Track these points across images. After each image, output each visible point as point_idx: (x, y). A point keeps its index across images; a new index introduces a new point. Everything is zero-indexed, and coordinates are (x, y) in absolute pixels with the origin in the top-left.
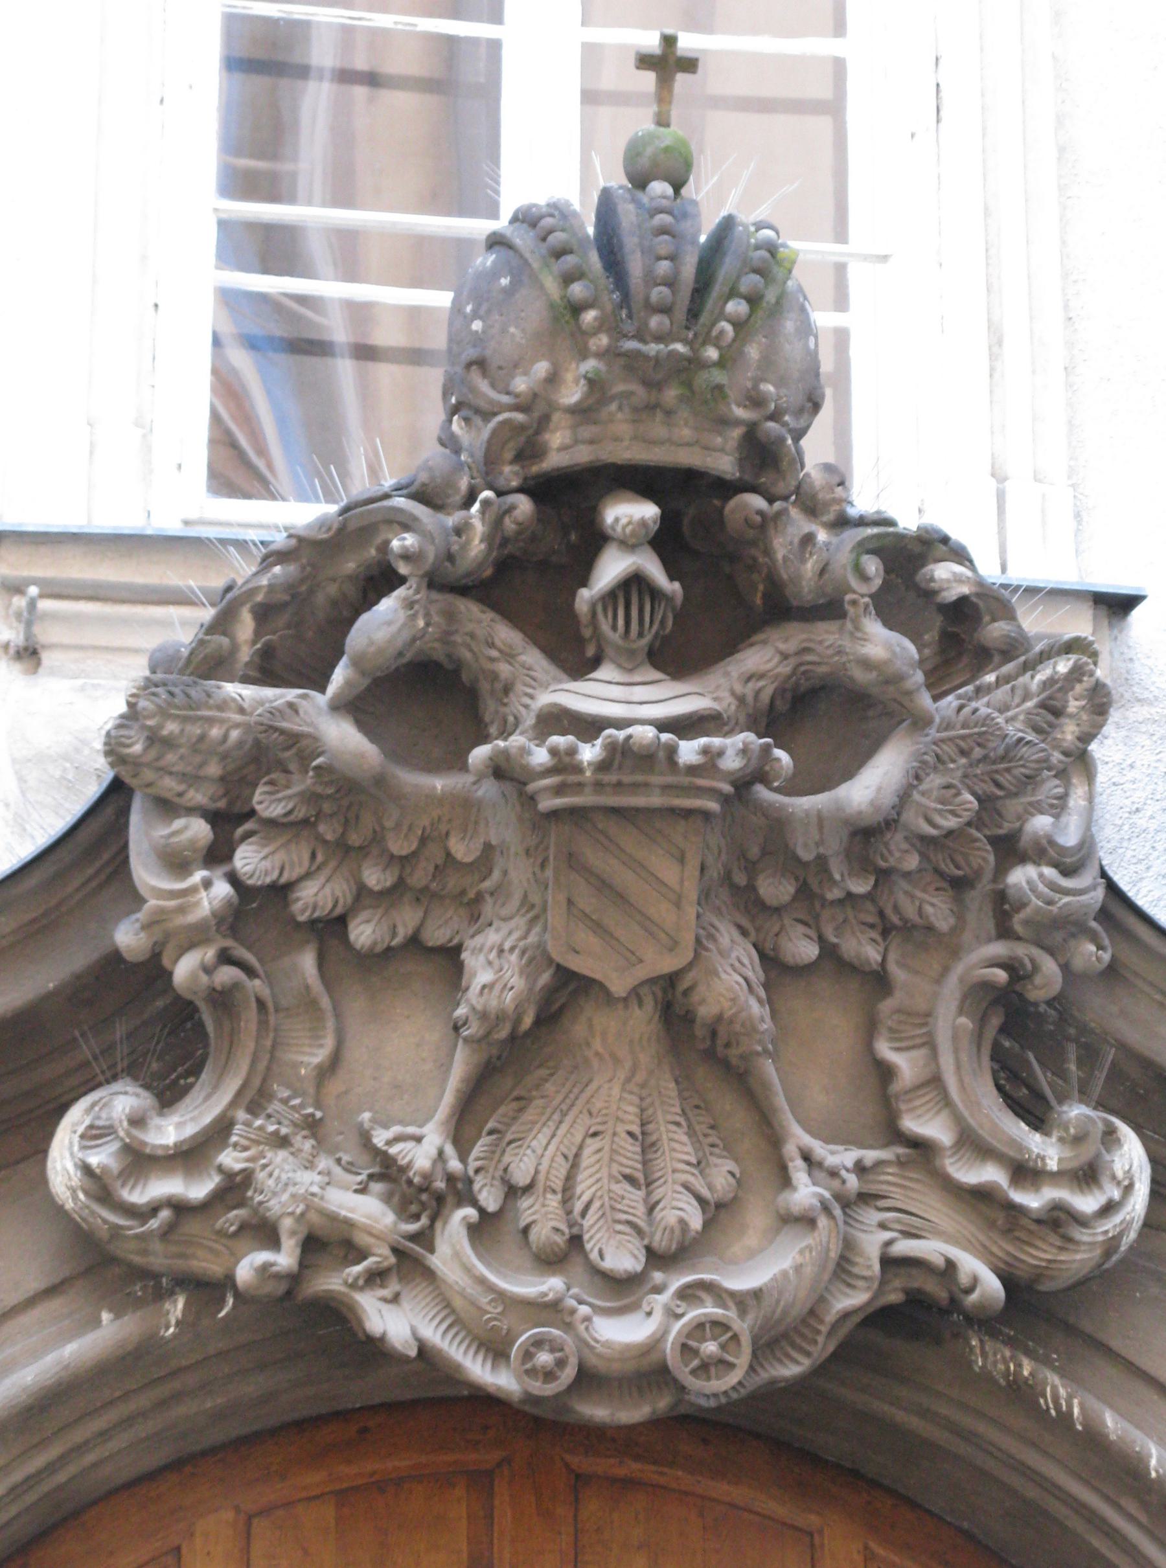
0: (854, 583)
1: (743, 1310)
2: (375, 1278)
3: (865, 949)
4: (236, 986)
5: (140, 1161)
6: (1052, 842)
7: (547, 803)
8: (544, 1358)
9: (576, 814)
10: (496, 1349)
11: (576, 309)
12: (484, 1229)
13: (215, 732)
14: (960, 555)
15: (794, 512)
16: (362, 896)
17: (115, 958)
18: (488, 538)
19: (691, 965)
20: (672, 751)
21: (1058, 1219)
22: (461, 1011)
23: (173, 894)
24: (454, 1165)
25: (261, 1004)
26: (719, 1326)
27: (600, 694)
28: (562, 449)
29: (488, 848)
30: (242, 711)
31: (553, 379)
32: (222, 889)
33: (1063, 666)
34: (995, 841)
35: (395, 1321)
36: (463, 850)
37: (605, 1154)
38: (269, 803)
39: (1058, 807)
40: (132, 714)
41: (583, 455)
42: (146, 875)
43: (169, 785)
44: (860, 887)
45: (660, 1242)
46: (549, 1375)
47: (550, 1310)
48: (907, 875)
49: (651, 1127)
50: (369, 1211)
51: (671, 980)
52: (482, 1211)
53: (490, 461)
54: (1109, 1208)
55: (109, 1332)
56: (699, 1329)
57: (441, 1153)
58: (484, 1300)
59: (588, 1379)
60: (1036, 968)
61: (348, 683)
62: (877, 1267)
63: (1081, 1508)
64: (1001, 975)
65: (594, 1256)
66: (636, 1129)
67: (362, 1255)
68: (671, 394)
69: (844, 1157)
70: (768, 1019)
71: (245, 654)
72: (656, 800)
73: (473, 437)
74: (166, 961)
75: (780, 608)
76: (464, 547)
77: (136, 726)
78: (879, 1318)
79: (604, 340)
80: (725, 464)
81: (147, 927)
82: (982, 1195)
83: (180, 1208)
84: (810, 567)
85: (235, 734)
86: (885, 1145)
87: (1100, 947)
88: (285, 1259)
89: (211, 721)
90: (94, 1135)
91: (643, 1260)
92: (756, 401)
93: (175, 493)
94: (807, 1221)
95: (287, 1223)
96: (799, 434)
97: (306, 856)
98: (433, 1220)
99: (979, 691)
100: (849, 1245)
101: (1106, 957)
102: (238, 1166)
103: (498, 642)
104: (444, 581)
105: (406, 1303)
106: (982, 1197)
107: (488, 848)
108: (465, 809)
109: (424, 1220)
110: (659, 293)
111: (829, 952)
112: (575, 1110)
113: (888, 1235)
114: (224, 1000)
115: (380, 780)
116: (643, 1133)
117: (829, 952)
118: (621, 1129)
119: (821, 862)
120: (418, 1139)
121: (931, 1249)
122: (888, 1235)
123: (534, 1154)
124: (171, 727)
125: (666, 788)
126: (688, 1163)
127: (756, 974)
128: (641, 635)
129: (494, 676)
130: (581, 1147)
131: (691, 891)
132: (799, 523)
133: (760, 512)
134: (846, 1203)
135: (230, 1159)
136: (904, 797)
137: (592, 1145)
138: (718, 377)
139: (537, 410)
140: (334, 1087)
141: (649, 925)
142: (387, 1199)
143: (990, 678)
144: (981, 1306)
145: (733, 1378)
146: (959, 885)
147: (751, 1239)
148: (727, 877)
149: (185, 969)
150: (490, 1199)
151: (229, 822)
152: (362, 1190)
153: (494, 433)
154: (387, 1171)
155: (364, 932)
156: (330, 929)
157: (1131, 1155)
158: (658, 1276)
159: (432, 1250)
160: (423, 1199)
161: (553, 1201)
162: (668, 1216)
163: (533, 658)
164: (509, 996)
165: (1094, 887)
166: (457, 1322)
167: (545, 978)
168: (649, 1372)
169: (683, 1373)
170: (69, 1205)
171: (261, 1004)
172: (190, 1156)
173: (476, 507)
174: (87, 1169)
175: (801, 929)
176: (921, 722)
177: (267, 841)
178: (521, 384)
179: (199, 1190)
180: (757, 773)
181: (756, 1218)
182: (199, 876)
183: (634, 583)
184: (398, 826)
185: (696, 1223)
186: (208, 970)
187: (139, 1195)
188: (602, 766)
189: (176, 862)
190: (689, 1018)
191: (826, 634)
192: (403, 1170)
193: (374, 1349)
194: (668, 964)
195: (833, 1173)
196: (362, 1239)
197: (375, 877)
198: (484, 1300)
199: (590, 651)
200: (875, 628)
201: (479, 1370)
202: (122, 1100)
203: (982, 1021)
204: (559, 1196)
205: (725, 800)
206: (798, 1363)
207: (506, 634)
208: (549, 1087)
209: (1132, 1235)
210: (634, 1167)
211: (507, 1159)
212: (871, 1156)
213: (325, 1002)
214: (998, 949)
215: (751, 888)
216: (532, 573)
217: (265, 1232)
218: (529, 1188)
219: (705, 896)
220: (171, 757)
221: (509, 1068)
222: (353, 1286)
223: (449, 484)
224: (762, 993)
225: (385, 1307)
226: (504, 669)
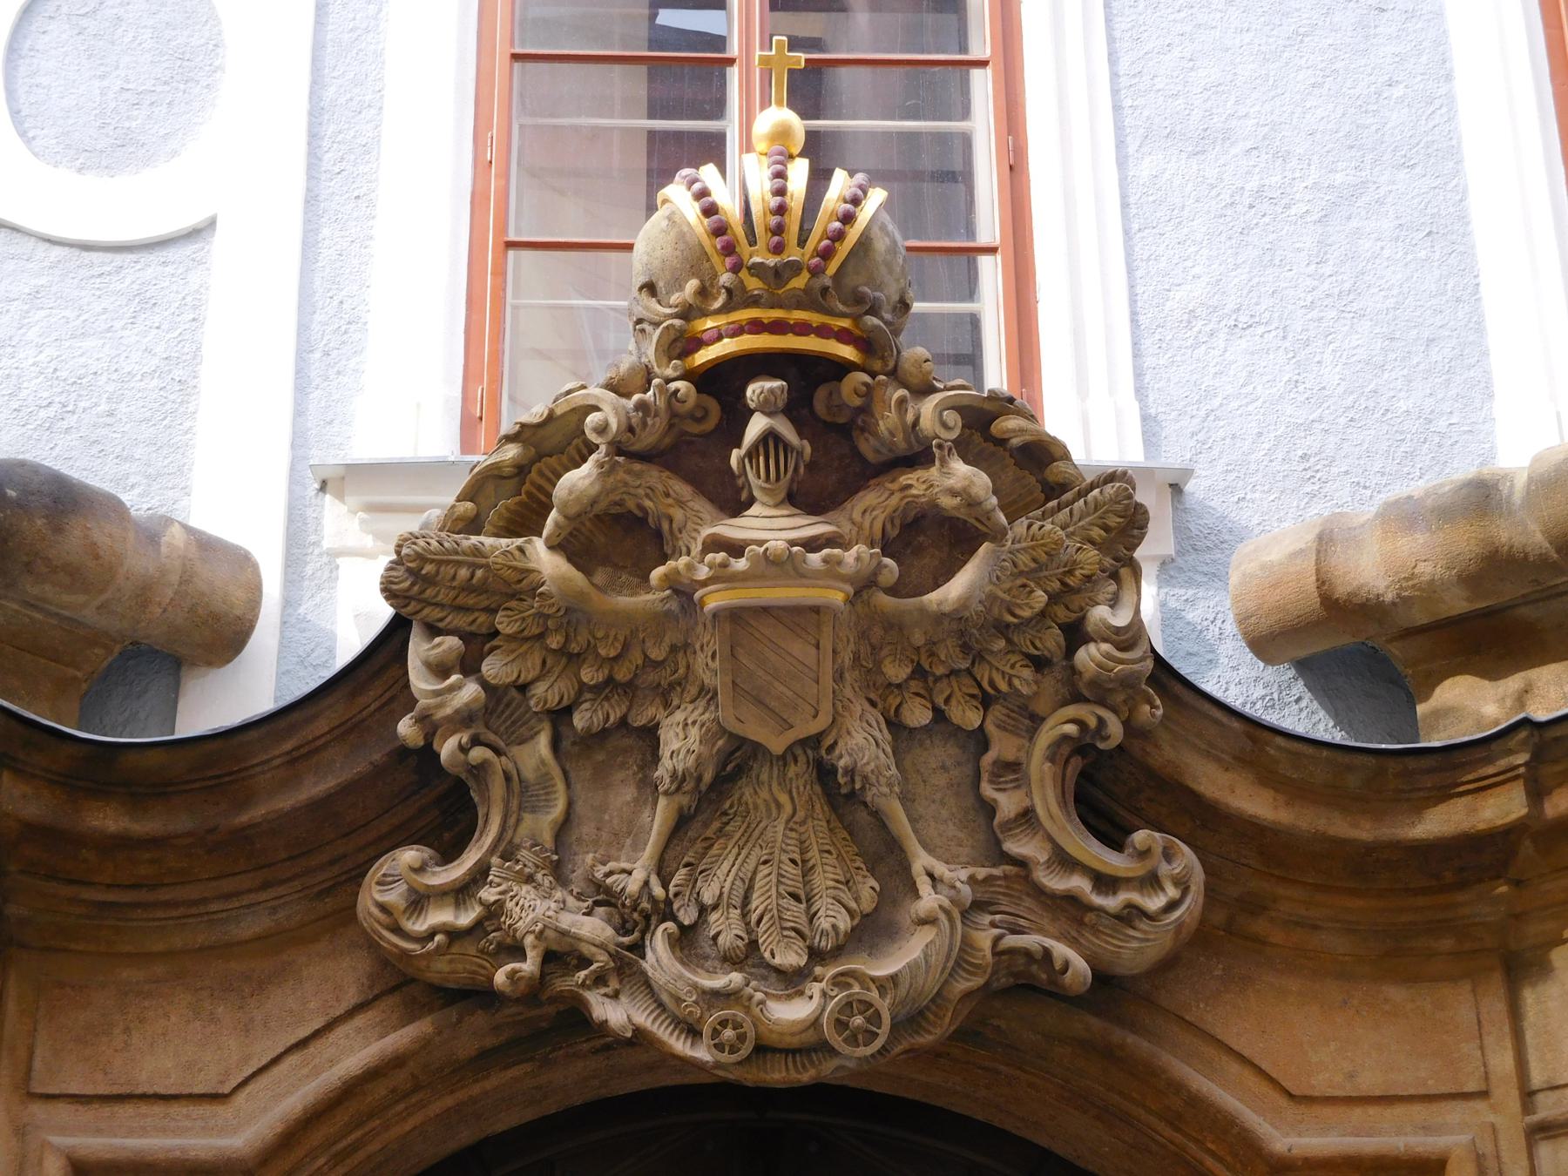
1: (882, 989)
2: (599, 980)
5: (419, 901)
10: (693, 1032)
13: (464, 573)
21: (1131, 915)
23: (437, 693)
24: (658, 891)
35: (615, 1012)
37: (773, 877)
39: (1114, 602)
42: (420, 682)
43: (432, 614)
49: (810, 855)
50: (593, 928)
51: (814, 741)
52: (681, 926)
57: (646, 883)
61: (557, 524)
62: (988, 953)
65: (767, 955)
66: (797, 857)
67: (585, 962)
70: (893, 768)
74: (435, 746)
77: (402, 569)
82: (1071, 900)
83: (454, 934)
86: (994, 866)
87: (1153, 706)
88: (529, 966)
91: (806, 958)
95: (529, 940)
96: (896, 333)
97: (538, 662)
98: (643, 933)
99: (1044, 517)
101: (1160, 712)
102: (492, 899)
105: (623, 998)
109: (636, 934)
111: (939, 715)
112: (750, 845)
113: (997, 931)
114: (480, 770)
116: (804, 861)
117: (939, 715)
118: (784, 858)
122: (997, 931)
126: (837, 881)
128: (778, 479)
130: (755, 873)
133: (866, 384)
135: (488, 894)
137: (764, 870)
142: (609, 921)
146: (1039, 664)
149: (447, 749)
150: (688, 916)
156: (560, 716)
158: (818, 970)
159: (643, 957)
160: (635, 919)
162: (824, 923)
163: (701, 506)
165: (1142, 659)
169: (836, 1041)
172: (461, 893)
175: (918, 699)
176: (998, 536)
178: (675, 298)
179: (466, 919)
182: (454, 678)
184: (607, 636)
186: (463, 749)
187: (420, 926)
189: (440, 670)
190: (833, 771)
194: (814, 728)
196: (586, 950)
197: (588, 675)
199: (744, 496)
201: (680, 1045)
202: (409, 855)
204: (738, 911)
206: (930, 1033)
207: (681, 489)
211: (699, 884)
214: (1071, 711)
216: (691, 438)
224: (889, 750)
225: (607, 1000)
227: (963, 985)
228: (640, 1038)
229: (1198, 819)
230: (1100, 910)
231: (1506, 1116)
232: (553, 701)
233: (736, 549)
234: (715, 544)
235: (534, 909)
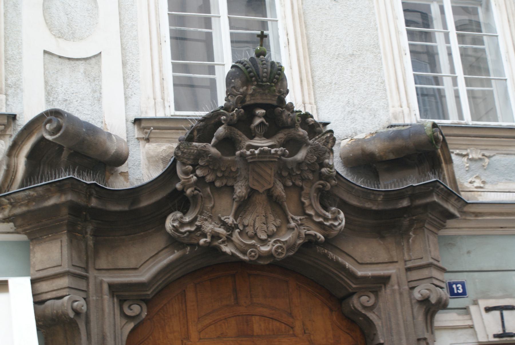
0: (297, 122)
1: (284, 244)
2: (223, 242)
3: (299, 183)
4: (198, 194)
6: (329, 164)
7: (249, 161)
8: (253, 254)
9: (254, 162)
10: (244, 253)
11: (252, 77)
12: (240, 233)
13: (192, 151)
14: (312, 117)
15: (286, 111)
16: (217, 178)
17: (176, 189)
18: (237, 116)
19: (272, 187)
20: (270, 151)
21: (332, 226)
22: (235, 196)
24: (235, 222)
25: (201, 197)
26: (281, 247)
27: (256, 142)
28: (249, 101)
29: (238, 168)
30: (196, 147)
31: (247, 89)
32: (195, 178)
33: (328, 135)
34: (319, 164)
35: (227, 249)
36: (233, 169)
38: (201, 163)
40: (178, 148)
41: (252, 102)
42: (180, 175)
43: (185, 160)
44: (298, 173)
45: (269, 233)
46: (254, 257)
47: (253, 246)
48: (305, 170)
50: (221, 231)
53: (237, 103)
54: (340, 224)
55: (176, 255)
56: (278, 248)
57: (233, 222)
58: (242, 245)
60: (327, 185)
61: (215, 142)
63: (335, 274)
64: (321, 186)
67: (221, 238)
68: (267, 91)
69: (298, 218)
71: (196, 138)
72: (268, 159)
73: (233, 100)
74: (185, 190)
75: (285, 126)
76: (234, 118)
78: (304, 245)
79: (256, 83)
80: (275, 103)
81: (182, 184)
83: (190, 232)
84: (289, 120)
85: (195, 151)
88: (208, 240)
89: (191, 149)
90: (174, 221)
93: (169, 110)
94: (293, 229)
95: (209, 233)
98: (232, 232)
99: (316, 139)
100: (299, 233)
103: (239, 134)
106: (320, 224)
107: (238, 168)
108: (234, 162)
110: (265, 74)
111: (294, 184)
115: (220, 158)
117: (294, 184)
119: (292, 169)
120: (229, 218)
121: (312, 232)
123: (248, 220)
124: (186, 150)
125: (269, 157)
127: (282, 188)
129: (238, 140)
131: (273, 175)
132: (287, 113)
135: (198, 223)
137: (257, 218)
138: (275, 88)
139: (244, 94)
140: (214, 210)
142: (224, 229)
143: (317, 137)
144: (321, 241)
145: (283, 255)
146: (313, 172)
147: (283, 232)
148: (277, 172)
149: (189, 191)
151: (195, 165)
152: (220, 227)
153: (237, 100)
154: (224, 224)
155: (218, 184)
156: (212, 184)
157: (342, 215)
158: (269, 239)
159: (232, 237)
160: (230, 228)
161: (252, 228)
162: (271, 229)
164: (244, 194)
166: (237, 249)
167: (249, 190)
168: (270, 255)
170: (170, 232)
171: (201, 197)
173: (234, 111)
174: (173, 226)
176: (308, 144)
177: (201, 169)
178: (241, 90)
179: (193, 229)
180: (283, 155)
181: (284, 229)
183: (262, 123)
185: (275, 230)
186: (193, 191)
187: (183, 230)
188: (259, 154)
189: (186, 173)
191: (292, 131)
192: (227, 224)
193: (225, 253)
194: (269, 187)
195: (297, 221)
196: (221, 236)
197: (219, 175)
198: (242, 245)
200: (300, 129)
203: (318, 194)
205: (278, 159)
207: (240, 133)
208: (250, 209)
209: (343, 228)
210: (264, 221)
212: (302, 217)
213: (212, 196)
215: (281, 173)
217: (204, 235)
218: (247, 226)
220: (185, 155)
221: (243, 206)
222: (220, 244)
223: (230, 107)
226: (240, 138)
227: (300, 242)
228: (233, 255)
229: (344, 205)
230: (326, 225)
231: (401, 266)
232: (211, 180)
233: (256, 148)
234: (250, 147)
235: (209, 227)
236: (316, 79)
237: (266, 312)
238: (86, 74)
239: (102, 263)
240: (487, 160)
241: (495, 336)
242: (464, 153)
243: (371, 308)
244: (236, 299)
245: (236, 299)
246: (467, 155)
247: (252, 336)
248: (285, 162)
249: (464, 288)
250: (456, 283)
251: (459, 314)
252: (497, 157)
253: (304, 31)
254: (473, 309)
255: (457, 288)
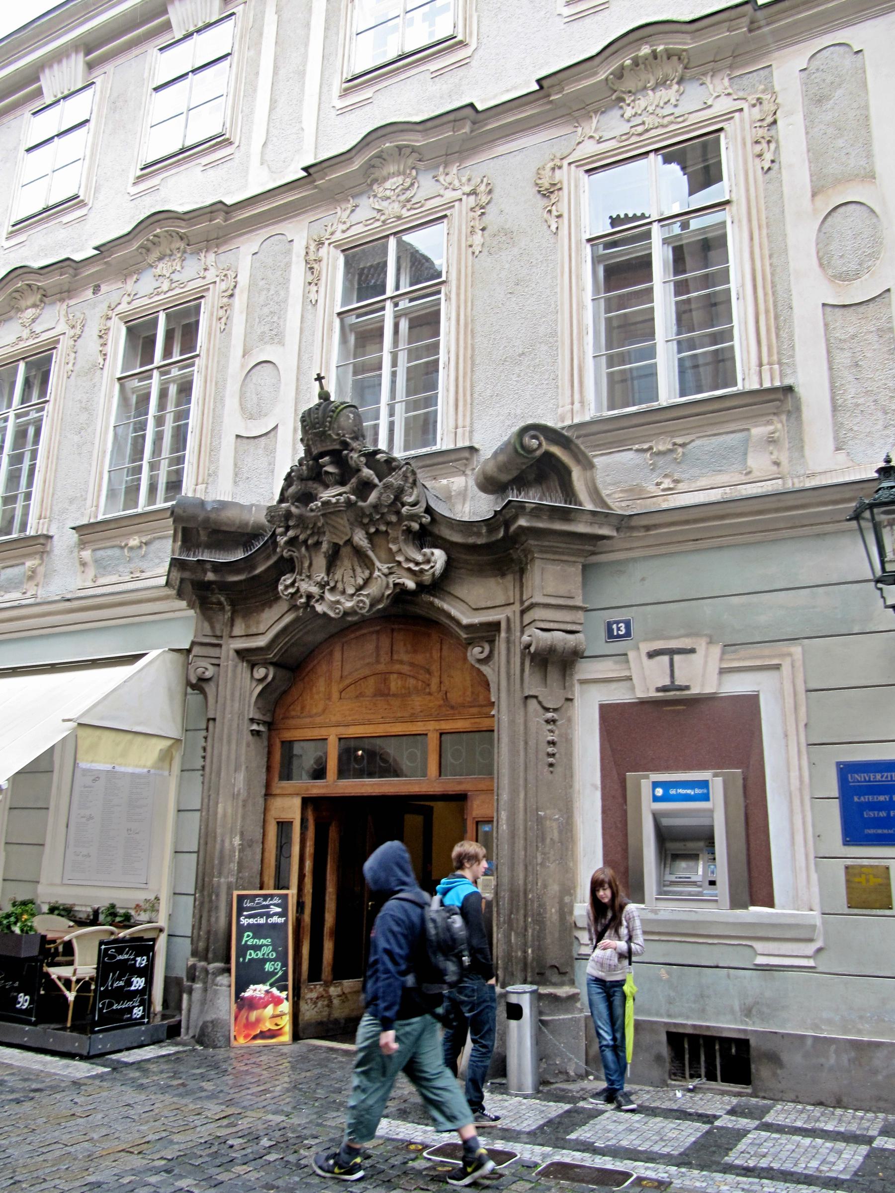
2: (317, 601)
3: (383, 528)
21: (422, 571)
28: (315, 452)
35: (320, 608)
38: (291, 523)
50: (314, 590)
56: (358, 602)
59: (346, 614)
80: (337, 447)
92: (338, 435)
104: (302, 479)
123: (338, 576)
134: (386, 575)
136: (379, 498)
141: (343, 532)
150: (332, 584)
155: (310, 542)
160: (322, 586)
163: (321, 489)
176: (375, 486)
217: (301, 597)
219: (351, 524)
227: (388, 592)
228: (325, 614)
231: (517, 608)
236: (475, 396)
237: (406, 669)
238: (266, 448)
239: (238, 630)
240: (680, 450)
241: (658, 690)
242: (646, 446)
243: (486, 660)
244: (378, 655)
245: (378, 655)
246: (651, 448)
247: (388, 695)
248: (362, 508)
249: (628, 627)
250: (617, 623)
251: (616, 662)
252: (698, 442)
253: (469, 342)
254: (632, 655)
255: (619, 629)
